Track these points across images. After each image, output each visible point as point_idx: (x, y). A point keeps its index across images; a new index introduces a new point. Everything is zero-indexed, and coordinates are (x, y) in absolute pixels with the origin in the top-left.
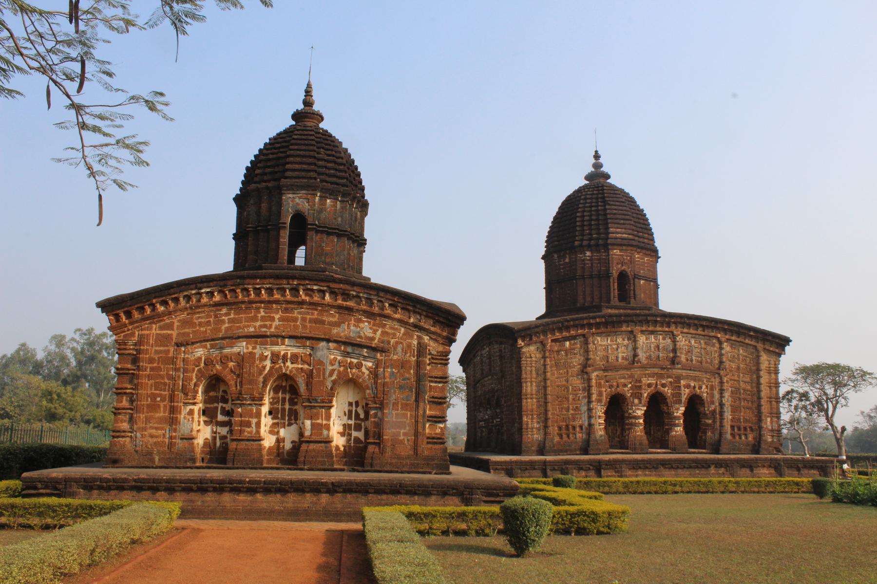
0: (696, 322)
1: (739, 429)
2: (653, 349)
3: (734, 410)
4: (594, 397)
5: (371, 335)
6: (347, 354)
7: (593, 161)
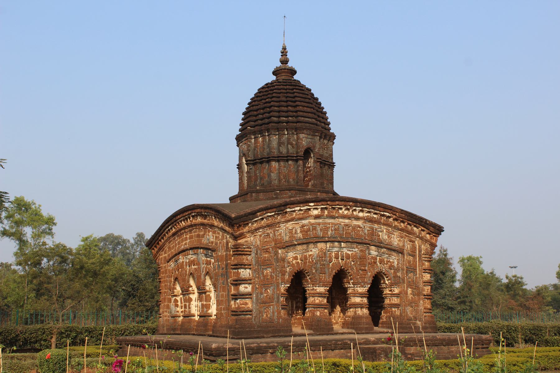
5: (212, 240)
6: (206, 255)
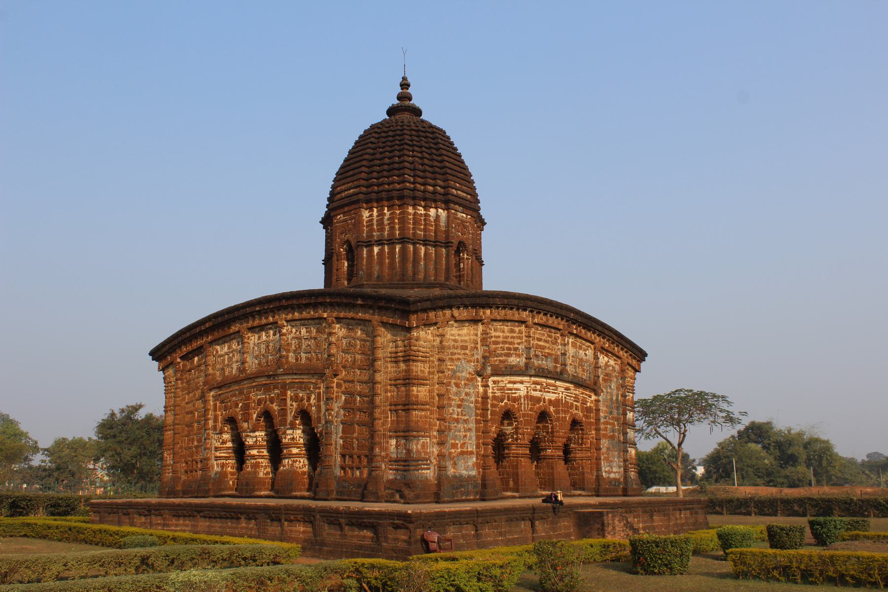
0: (295, 302)
1: (351, 456)
2: (263, 351)
3: (348, 426)
4: (211, 423)
7: (399, 90)
